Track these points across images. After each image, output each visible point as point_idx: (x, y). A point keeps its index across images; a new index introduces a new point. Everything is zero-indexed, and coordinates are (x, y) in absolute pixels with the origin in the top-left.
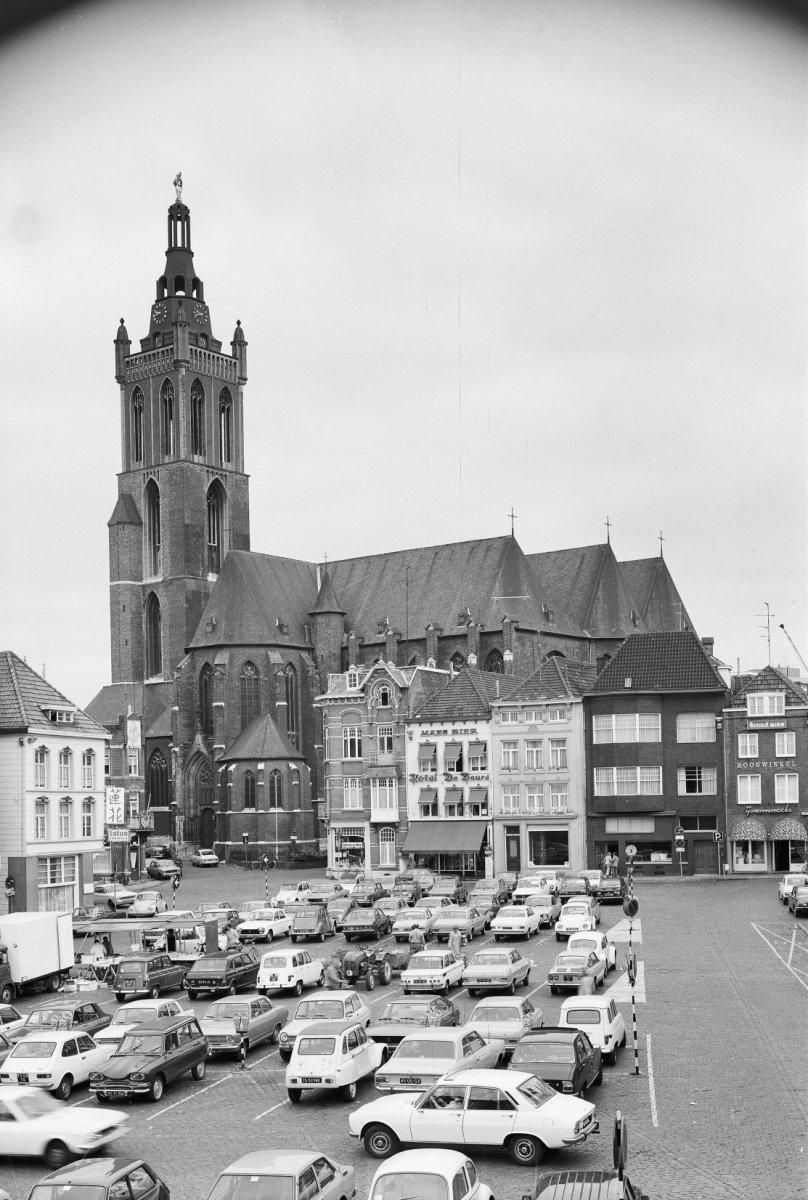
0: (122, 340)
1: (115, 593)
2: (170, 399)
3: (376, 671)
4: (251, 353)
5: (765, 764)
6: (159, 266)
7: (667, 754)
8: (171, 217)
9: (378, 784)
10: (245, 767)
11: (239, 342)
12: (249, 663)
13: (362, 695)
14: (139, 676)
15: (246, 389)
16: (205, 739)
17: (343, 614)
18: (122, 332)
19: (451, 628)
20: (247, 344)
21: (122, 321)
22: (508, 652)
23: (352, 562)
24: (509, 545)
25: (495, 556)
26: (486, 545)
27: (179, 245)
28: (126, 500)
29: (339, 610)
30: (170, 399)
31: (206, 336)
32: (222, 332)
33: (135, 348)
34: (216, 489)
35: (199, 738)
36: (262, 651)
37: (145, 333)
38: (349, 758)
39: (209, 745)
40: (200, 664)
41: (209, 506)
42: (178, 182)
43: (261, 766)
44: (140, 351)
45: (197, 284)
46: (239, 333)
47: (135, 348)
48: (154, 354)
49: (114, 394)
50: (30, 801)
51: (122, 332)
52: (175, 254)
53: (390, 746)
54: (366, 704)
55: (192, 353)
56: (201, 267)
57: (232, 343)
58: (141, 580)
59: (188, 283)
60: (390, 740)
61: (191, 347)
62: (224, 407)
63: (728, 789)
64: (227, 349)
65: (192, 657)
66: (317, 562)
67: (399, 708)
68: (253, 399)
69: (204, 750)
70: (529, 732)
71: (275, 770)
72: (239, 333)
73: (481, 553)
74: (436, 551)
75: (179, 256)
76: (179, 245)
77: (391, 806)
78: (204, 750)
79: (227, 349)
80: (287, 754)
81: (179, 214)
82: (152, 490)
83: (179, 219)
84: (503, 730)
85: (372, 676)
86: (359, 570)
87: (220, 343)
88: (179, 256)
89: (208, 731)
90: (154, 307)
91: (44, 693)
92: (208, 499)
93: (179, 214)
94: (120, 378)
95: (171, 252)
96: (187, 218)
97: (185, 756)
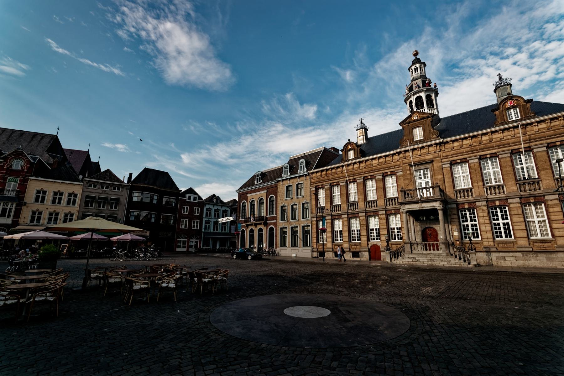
5: (190, 216)
7: (158, 208)
25: (46, 141)
26: (44, 136)
54: (3, 166)
63: (177, 222)
70: (102, 193)
74: (13, 131)
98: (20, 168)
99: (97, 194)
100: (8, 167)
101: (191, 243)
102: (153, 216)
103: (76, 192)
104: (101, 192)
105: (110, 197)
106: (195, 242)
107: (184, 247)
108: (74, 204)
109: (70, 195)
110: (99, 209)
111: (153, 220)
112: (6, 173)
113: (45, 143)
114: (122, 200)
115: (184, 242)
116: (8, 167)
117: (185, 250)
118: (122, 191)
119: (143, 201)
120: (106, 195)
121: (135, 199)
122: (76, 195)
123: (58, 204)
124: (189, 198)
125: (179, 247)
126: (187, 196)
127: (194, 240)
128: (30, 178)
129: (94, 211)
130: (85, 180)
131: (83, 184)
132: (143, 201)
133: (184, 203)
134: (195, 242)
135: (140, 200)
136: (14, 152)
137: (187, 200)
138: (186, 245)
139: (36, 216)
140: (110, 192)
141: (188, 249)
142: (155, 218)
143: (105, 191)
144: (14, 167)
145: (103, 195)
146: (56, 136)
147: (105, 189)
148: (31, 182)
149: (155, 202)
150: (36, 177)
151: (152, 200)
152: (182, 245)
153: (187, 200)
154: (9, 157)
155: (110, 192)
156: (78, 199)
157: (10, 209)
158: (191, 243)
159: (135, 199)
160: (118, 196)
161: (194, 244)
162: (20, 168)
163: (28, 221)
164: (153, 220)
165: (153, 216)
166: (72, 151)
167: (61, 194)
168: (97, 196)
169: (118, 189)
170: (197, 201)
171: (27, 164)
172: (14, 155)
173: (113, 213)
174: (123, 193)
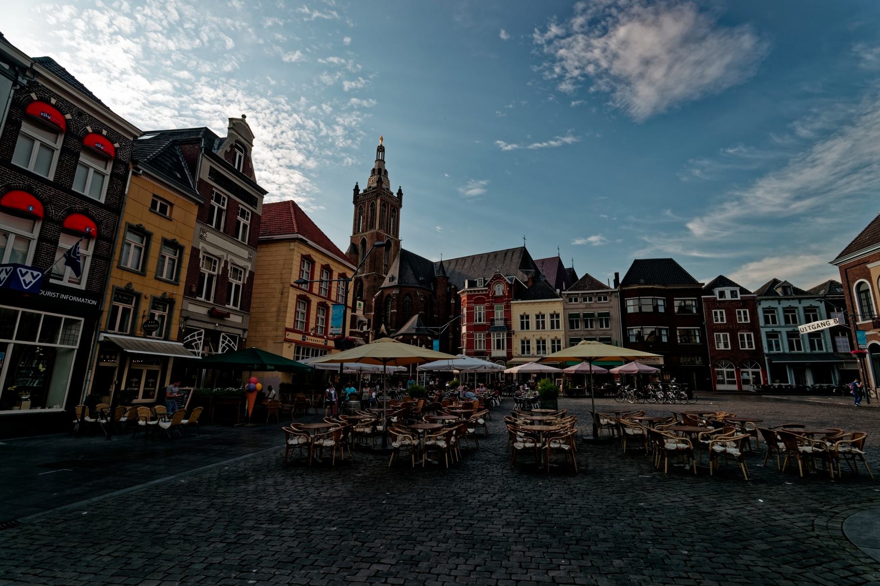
0: (356, 189)
4: (404, 197)
6: (373, 165)
7: (668, 319)
8: (378, 150)
9: (495, 336)
11: (400, 193)
13: (487, 288)
16: (386, 327)
18: (357, 187)
24: (524, 252)
26: (514, 251)
27: (380, 158)
31: (388, 189)
32: (394, 191)
33: (361, 192)
36: (414, 289)
37: (365, 187)
42: (382, 139)
45: (386, 171)
46: (400, 190)
47: (361, 192)
49: (352, 207)
51: (357, 187)
52: (377, 162)
54: (489, 294)
56: (387, 167)
57: (397, 194)
59: (383, 173)
64: (395, 195)
68: (403, 212)
69: (385, 332)
70: (586, 308)
72: (400, 190)
73: (510, 254)
74: (489, 255)
75: (381, 161)
77: (503, 349)
79: (395, 195)
81: (381, 149)
82: (364, 242)
84: (571, 307)
87: (392, 194)
88: (381, 161)
90: (369, 180)
93: (381, 149)
94: (355, 202)
95: (377, 160)
96: (384, 151)
98: (501, 294)
101: (745, 375)
102: (664, 332)
103: (557, 312)
104: (584, 306)
105: (596, 312)
106: (753, 373)
107: (733, 383)
108: (558, 327)
109: (552, 316)
110: (586, 331)
111: (665, 339)
112: (492, 302)
113: (517, 259)
114: (612, 313)
115: (730, 375)
117: (735, 387)
118: (610, 301)
119: (643, 310)
120: (593, 310)
121: (630, 310)
122: (558, 316)
123: (542, 328)
124: (722, 294)
125: (722, 382)
126: (717, 291)
127: (750, 370)
128: (512, 302)
129: (582, 333)
130: (564, 294)
131: (562, 299)
132: (643, 310)
133: (714, 304)
134: (753, 373)
136: (494, 277)
137: (718, 299)
138: (736, 379)
139: (525, 345)
140: (595, 305)
141: (740, 387)
142: (667, 335)
143: (589, 304)
144: (497, 294)
145: (586, 310)
146: (524, 247)
147: (588, 302)
148: (514, 307)
149: (661, 310)
150: (517, 300)
152: (726, 379)
153: (718, 299)
155: (595, 305)
156: (561, 319)
157: (503, 340)
158: (745, 376)
159: (630, 310)
160: (606, 309)
161: (751, 377)
162: (501, 294)
163: (520, 352)
164: (665, 339)
165: (664, 332)
166: (543, 261)
167: (543, 316)
168: (582, 312)
169: (605, 299)
170: (739, 298)
172: (495, 280)
173: (605, 334)
174: (611, 304)
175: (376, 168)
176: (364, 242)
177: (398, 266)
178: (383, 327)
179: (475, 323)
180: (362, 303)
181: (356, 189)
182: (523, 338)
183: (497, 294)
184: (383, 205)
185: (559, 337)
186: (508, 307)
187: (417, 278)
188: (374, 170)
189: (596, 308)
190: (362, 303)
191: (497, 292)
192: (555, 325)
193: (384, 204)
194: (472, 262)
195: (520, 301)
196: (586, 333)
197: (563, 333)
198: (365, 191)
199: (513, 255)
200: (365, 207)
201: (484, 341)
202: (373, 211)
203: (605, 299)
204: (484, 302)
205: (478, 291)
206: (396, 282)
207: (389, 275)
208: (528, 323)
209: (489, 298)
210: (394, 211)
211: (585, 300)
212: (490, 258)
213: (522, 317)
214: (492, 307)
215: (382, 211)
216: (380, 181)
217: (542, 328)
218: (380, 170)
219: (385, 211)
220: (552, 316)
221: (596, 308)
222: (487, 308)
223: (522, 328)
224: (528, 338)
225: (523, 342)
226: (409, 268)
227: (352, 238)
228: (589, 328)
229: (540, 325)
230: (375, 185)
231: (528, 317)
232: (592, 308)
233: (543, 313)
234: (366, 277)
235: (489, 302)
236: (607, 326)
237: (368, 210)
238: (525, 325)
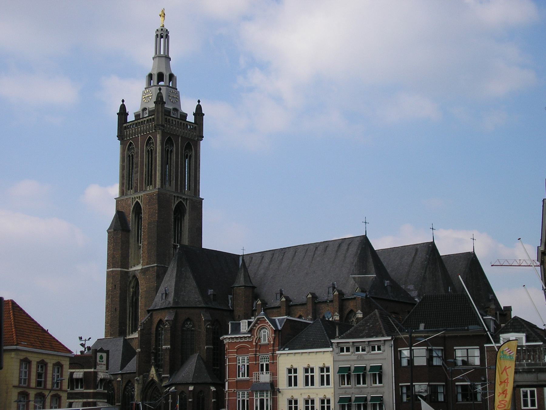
0: (123, 113)
1: (109, 275)
2: (151, 150)
3: (258, 320)
10: (181, 388)
11: (199, 113)
12: (188, 319)
13: (250, 335)
14: (122, 333)
15: (203, 144)
16: (157, 371)
17: (254, 287)
18: (123, 107)
19: (323, 295)
20: (204, 115)
21: (123, 101)
22: (359, 311)
23: (263, 254)
24: (364, 242)
25: (354, 249)
27: (162, 53)
28: (120, 216)
29: (251, 285)
30: (151, 150)
31: (176, 110)
33: (131, 118)
34: (180, 210)
35: (153, 371)
38: (241, 377)
39: (159, 375)
40: (156, 321)
41: (175, 219)
43: (191, 388)
44: (134, 119)
45: (171, 77)
46: (199, 108)
48: (142, 122)
50: (14, 395)
51: (123, 107)
52: (157, 59)
53: (267, 369)
55: (166, 121)
56: (175, 68)
57: (194, 114)
58: (128, 269)
60: (267, 365)
61: (166, 117)
62: (187, 155)
64: (191, 118)
65: (151, 316)
66: (240, 254)
67: (273, 344)
70: (358, 360)
71: (201, 391)
72: (199, 108)
73: (344, 247)
74: (316, 246)
76: (162, 53)
78: (156, 379)
79: (191, 118)
80: (209, 380)
82: (137, 209)
83: (162, 37)
84: (341, 358)
85: (256, 323)
86: (267, 260)
87: (184, 116)
89: (158, 367)
90: (144, 92)
91: (32, 327)
92: (174, 214)
94: (121, 136)
95: (157, 56)
96: (167, 36)
97: (144, 382)
99: (352, 363)
100: (257, 342)
102: (441, 390)
103: (327, 365)
105: (369, 364)
108: (328, 383)
114: (384, 368)
116: (257, 342)
122: (328, 370)
123: (311, 385)
128: (277, 352)
129: (353, 391)
131: (331, 349)
135: (479, 349)
143: (361, 355)
144: (262, 342)
148: (280, 358)
150: (284, 350)
151: (430, 359)
154: (255, 328)
155: (369, 357)
156: (331, 373)
157: (267, 400)
162: (267, 342)
165: (441, 390)
167: (312, 370)
168: (353, 365)
169: (379, 349)
171: (272, 334)
174: (385, 353)
175: (155, 73)
176: (137, 209)
177: (175, 274)
178: (153, 371)
179: (238, 378)
180: (104, 355)
181: (123, 113)
182: (290, 397)
183: (262, 342)
184: (168, 141)
185: (328, 396)
186: (274, 357)
187: (203, 293)
188: (150, 76)
189: (369, 360)
190: (104, 355)
191: (262, 339)
192: (325, 381)
193: (169, 139)
194: (293, 259)
195: (287, 351)
196: (357, 390)
197: (332, 390)
198: (137, 116)
199: (348, 249)
200: (137, 146)
201: (247, 401)
202: (151, 153)
203: (379, 349)
204: (249, 352)
205: (241, 338)
206: (171, 299)
207: (162, 289)
208: (296, 377)
209: (252, 346)
210: (188, 147)
211: (358, 349)
212: (318, 252)
213: (290, 371)
214: (256, 359)
215: (166, 154)
216: (159, 101)
217: (311, 385)
218: (161, 77)
219: (171, 151)
220: (322, 370)
221: (369, 360)
222: (249, 360)
223: (290, 385)
224: (295, 397)
225: (290, 402)
226: (192, 277)
227: (118, 201)
228: (362, 385)
229: (309, 381)
230: (152, 106)
231: (295, 371)
232: (366, 360)
233: (311, 366)
234: (144, 271)
235: (252, 352)
236: (380, 382)
237: (142, 152)
238: (292, 381)
